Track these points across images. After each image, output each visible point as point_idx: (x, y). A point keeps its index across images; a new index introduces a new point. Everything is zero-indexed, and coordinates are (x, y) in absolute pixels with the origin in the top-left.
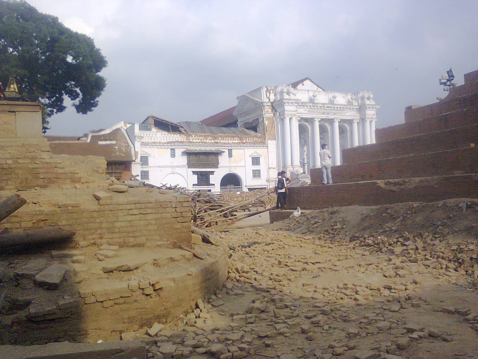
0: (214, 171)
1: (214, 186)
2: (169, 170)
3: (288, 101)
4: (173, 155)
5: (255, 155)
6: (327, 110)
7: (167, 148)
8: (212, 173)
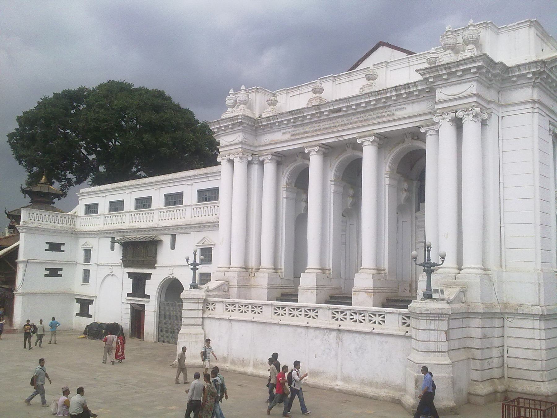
0: (151, 274)
1: (147, 300)
2: (107, 271)
3: (218, 126)
4: (113, 248)
5: (207, 245)
6: (340, 120)
7: (106, 237)
8: (148, 276)
